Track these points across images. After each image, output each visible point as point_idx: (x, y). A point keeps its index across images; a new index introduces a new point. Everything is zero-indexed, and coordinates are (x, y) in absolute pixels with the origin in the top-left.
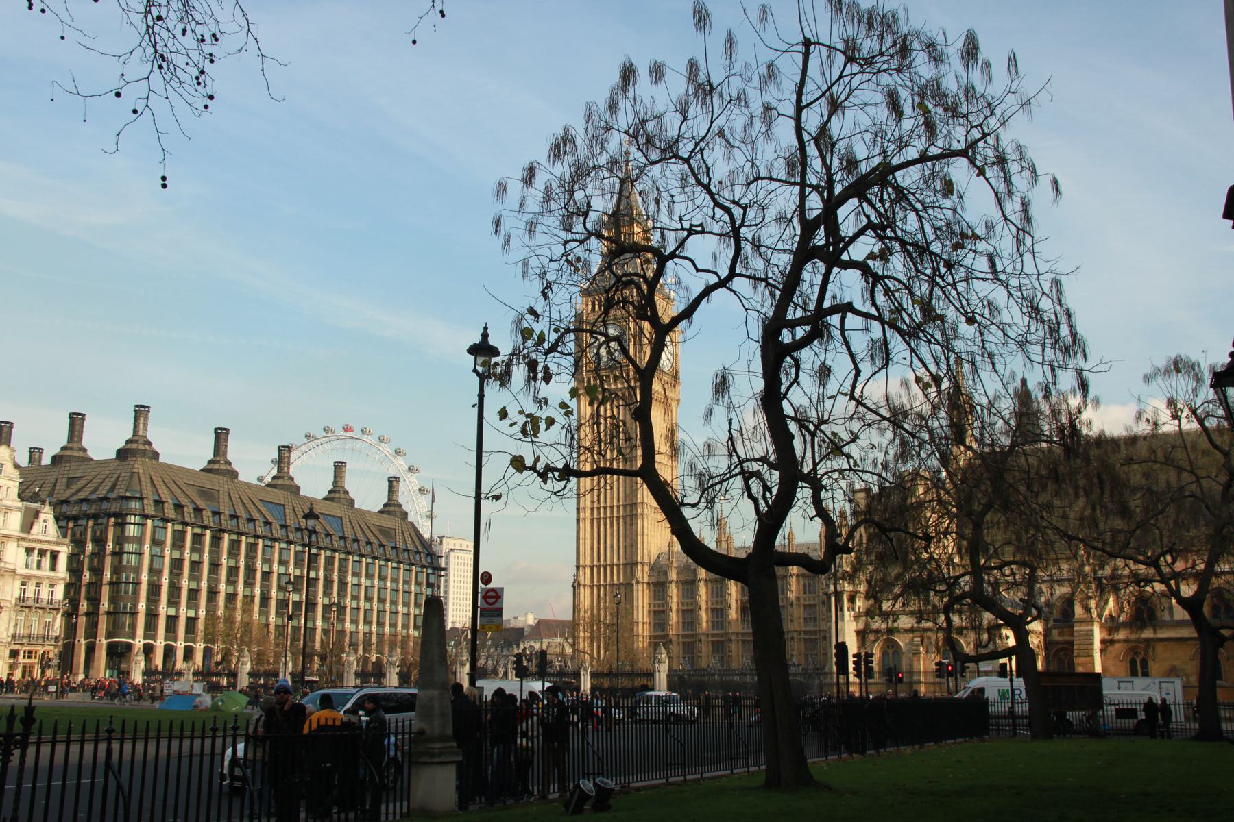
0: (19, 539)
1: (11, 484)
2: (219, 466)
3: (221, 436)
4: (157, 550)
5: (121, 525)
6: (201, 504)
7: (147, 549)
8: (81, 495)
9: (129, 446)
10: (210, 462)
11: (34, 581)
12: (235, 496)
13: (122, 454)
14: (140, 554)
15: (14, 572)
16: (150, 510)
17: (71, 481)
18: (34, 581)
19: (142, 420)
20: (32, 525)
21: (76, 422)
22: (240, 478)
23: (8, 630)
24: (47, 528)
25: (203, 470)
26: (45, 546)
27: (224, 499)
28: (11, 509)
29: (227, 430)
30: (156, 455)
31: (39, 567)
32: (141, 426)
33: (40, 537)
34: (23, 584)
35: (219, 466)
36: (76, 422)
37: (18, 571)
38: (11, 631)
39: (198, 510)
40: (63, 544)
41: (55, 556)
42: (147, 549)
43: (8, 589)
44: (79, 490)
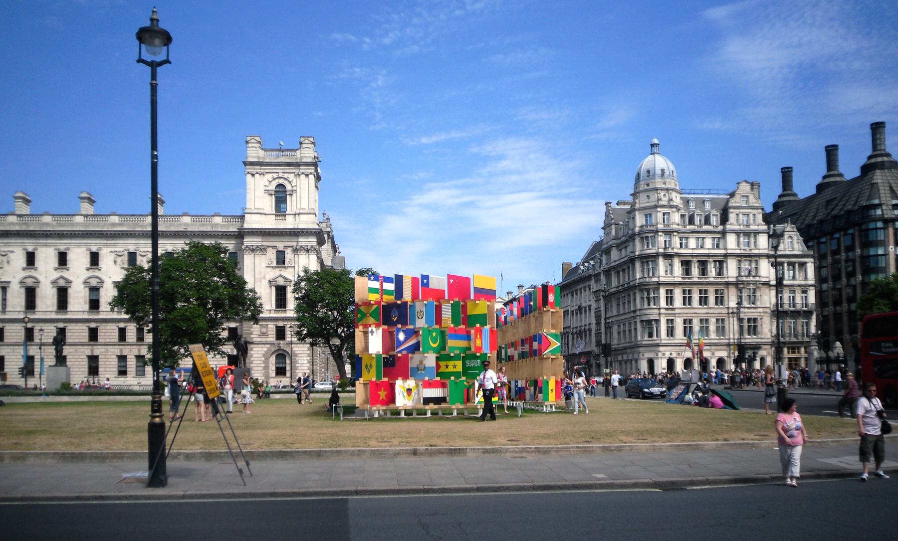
0: (768, 256)
1: (755, 211)
14: (886, 255)
17: (828, 202)
21: (831, 152)
28: (756, 233)
33: (788, 253)
41: (803, 265)
43: (766, 298)
44: (833, 209)
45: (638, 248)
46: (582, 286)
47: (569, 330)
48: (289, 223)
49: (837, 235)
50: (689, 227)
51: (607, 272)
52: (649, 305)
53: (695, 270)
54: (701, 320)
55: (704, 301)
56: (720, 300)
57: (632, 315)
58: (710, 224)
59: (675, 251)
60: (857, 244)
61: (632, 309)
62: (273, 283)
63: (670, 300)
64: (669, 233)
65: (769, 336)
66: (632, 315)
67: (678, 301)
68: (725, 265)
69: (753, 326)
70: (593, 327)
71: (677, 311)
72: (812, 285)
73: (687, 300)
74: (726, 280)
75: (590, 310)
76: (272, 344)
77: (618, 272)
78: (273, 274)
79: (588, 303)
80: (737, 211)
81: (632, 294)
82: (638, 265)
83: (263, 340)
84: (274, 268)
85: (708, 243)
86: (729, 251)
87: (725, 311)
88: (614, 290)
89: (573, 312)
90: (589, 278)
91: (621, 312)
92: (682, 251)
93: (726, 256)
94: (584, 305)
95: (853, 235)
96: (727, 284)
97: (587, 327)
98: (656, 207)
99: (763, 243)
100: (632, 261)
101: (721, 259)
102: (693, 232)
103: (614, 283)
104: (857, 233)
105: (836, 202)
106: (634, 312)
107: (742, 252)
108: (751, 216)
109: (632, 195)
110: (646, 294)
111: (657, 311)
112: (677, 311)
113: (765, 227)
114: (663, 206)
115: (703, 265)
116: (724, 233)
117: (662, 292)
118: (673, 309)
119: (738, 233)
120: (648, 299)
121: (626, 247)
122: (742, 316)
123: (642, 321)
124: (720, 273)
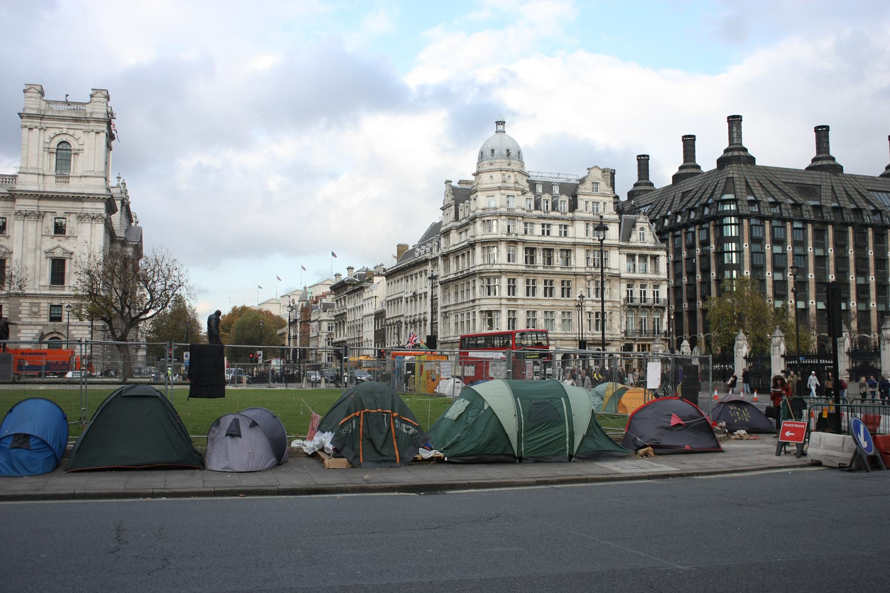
0: (620, 247)
1: (606, 199)
2: (824, 162)
3: (822, 133)
4: (756, 247)
5: (720, 227)
6: (800, 200)
7: (746, 246)
8: (690, 205)
9: (730, 154)
10: (814, 160)
11: (638, 283)
12: (839, 190)
13: (722, 162)
15: (618, 276)
16: (744, 210)
17: (684, 194)
18: (638, 283)
19: (735, 130)
20: (630, 236)
21: (689, 142)
22: (846, 171)
23: (620, 327)
24: (645, 234)
25: (808, 168)
26: (646, 252)
27: (826, 193)
29: (827, 127)
30: (752, 160)
31: (645, 272)
32: (735, 135)
33: (639, 244)
34: (629, 286)
35: (824, 162)
36: (689, 142)
37: (622, 275)
38: (624, 328)
39: (796, 206)
40: (661, 249)
41: (655, 258)
42: (746, 246)
43: (615, 291)
44: (689, 201)
45: (479, 231)
46: (417, 271)
47: (402, 319)
48: (74, 186)
49: (692, 229)
50: (535, 213)
51: (446, 256)
52: (489, 294)
53: (539, 259)
54: (546, 312)
55: (548, 291)
56: (566, 291)
57: (471, 304)
58: (558, 211)
59: (520, 237)
60: (712, 239)
61: (471, 298)
62: (50, 255)
63: (512, 289)
64: (512, 217)
65: (619, 332)
66: (471, 304)
67: (521, 292)
68: (573, 255)
69: (601, 320)
70: (429, 317)
71: (520, 302)
72: (664, 280)
73: (531, 290)
74: (574, 270)
75: (426, 297)
76: (44, 325)
77: (457, 257)
78: (50, 243)
79: (424, 290)
80: (587, 198)
81: (471, 281)
82: (478, 249)
83: (34, 321)
84: (52, 237)
85: (555, 230)
86: (578, 240)
87: (573, 304)
88: (453, 276)
89: (407, 298)
90: (426, 261)
91: (460, 301)
92: (527, 238)
93: (574, 244)
94: (419, 292)
95: (708, 229)
96: (575, 275)
97: (422, 317)
98: (500, 188)
99: (613, 234)
100: (472, 245)
101: (567, 247)
102: (540, 218)
103: (453, 268)
104: (712, 228)
105: (691, 194)
106: (473, 301)
107: (592, 241)
108: (601, 204)
109: (474, 175)
110: (486, 281)
111: (498, 302)
112: (520, 302)
113: (617, 217)
114: (508, 188)
115: (548, 252)
116: (573, 220)
117: (504, 280)
118: (515, 300)
119: (587, 222)
120: (489, 287)
121: (466, 230)
122: (589, 309)
123: (481, 312)
124: (567, 262)
